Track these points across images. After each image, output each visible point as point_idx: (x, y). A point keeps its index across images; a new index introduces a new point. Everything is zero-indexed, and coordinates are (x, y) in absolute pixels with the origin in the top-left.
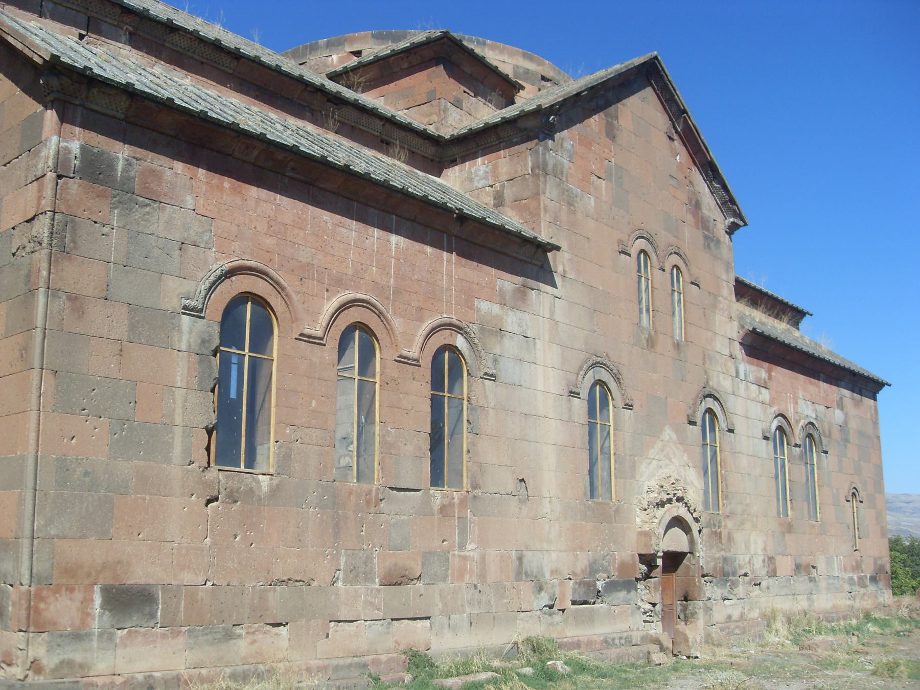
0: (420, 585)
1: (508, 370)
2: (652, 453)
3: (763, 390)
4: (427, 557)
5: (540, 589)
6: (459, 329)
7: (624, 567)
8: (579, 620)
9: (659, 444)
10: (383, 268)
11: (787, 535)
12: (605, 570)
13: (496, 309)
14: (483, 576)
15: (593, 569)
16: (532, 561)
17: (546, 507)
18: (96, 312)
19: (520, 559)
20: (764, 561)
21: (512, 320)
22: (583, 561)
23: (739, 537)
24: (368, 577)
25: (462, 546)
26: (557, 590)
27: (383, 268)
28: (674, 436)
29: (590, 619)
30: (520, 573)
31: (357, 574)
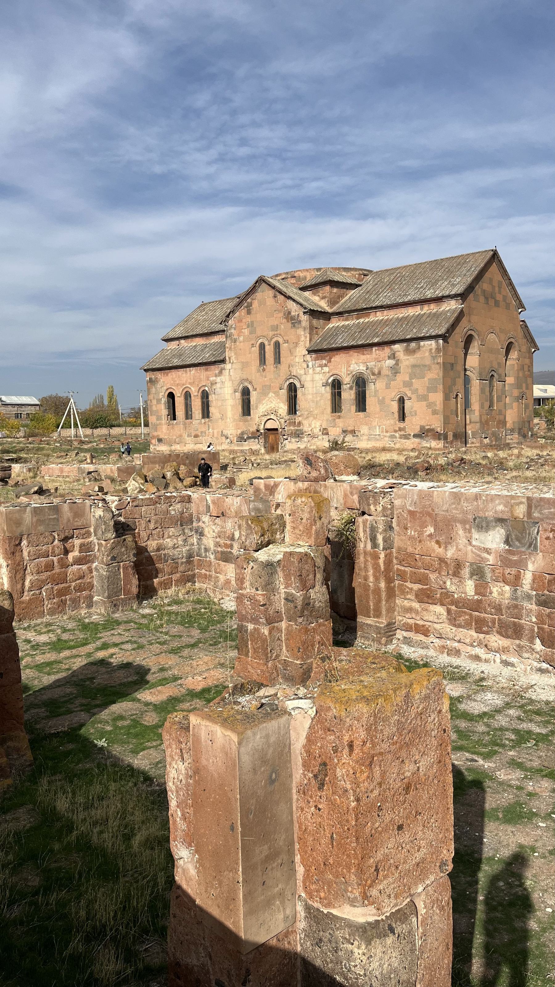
0: (201, 438)
1: (218, 391)
2: (264, 402)
3: (324, 368)
4: (202, 432)
5: (227, 438)
6: (205, 386)
7: (253, 433)
8: (238, 445)
9: (267, 399)
10: (190, 379)
11: (337, 420)
12: (246, 434)
13: (214, 378)
14: (213, 436)
15: (243, 433)
16: (225, 432)
17: (228, 420)
18: (153, 401)
19: (222, 432)
20: (320, 430)
21: (218, 379)
22: (239, 432)
23: (305, 423)
24: (191, 436)
25: (209, 430)
26: (232, 439)
27: (190, 379)
28: (273, 395)
29: (242, 445)
30: (222, 435)
31: (189, 436)
